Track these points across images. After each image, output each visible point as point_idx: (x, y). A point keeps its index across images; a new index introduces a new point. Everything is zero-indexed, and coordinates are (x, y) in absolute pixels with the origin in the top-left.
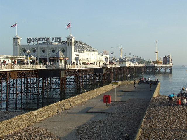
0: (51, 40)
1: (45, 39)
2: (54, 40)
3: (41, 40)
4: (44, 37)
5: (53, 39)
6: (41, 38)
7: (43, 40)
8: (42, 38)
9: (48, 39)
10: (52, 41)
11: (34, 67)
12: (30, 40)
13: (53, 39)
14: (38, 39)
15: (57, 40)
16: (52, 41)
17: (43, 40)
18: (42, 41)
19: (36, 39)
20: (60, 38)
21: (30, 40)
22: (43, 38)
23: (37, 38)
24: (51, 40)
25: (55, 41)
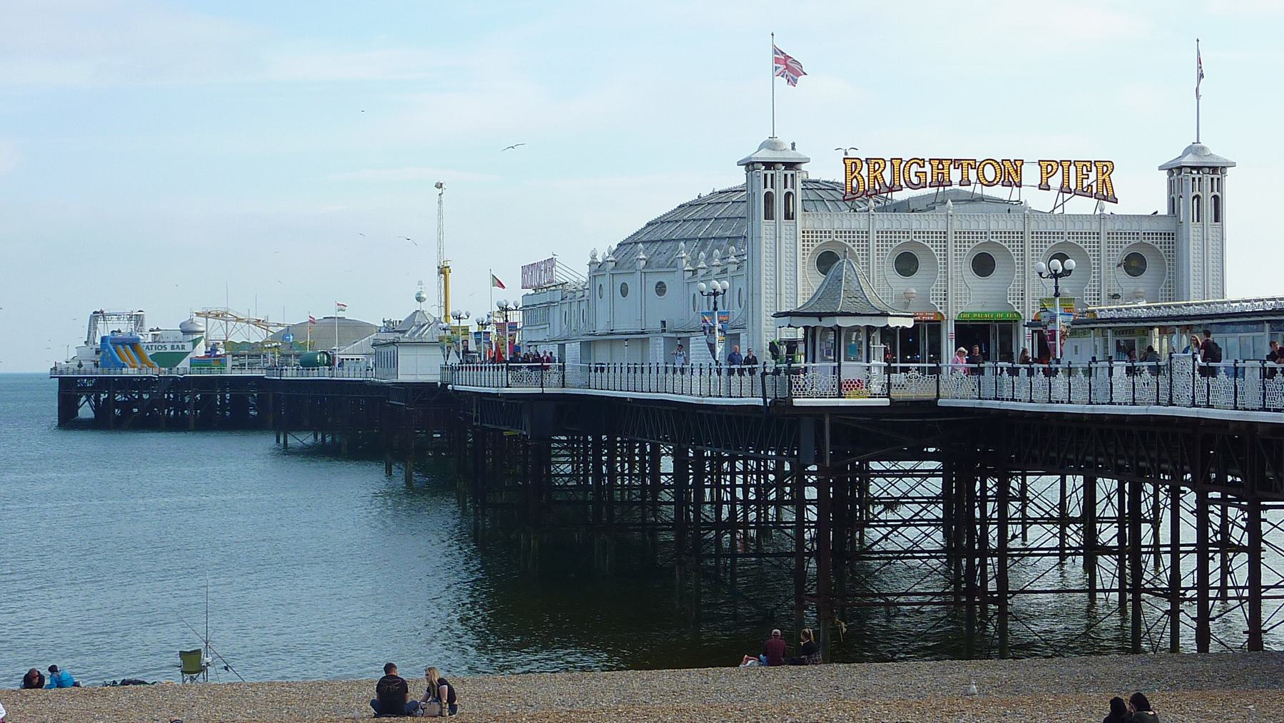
1: (990, 173)
3: (956, 175)
4: (979, 159)
5: (1048, 167)
6: (957, 163)
7: (973, 175)
9: (1010, 173)
11: (1100, 398)
12: (864, 172)
14: (928, 168)
18: (965, 182)
19: (915, 168)
20: (1106, 168)
21: (864, 172)
22: (973, 164)
23: (920, 162)
24: (1031, 175)
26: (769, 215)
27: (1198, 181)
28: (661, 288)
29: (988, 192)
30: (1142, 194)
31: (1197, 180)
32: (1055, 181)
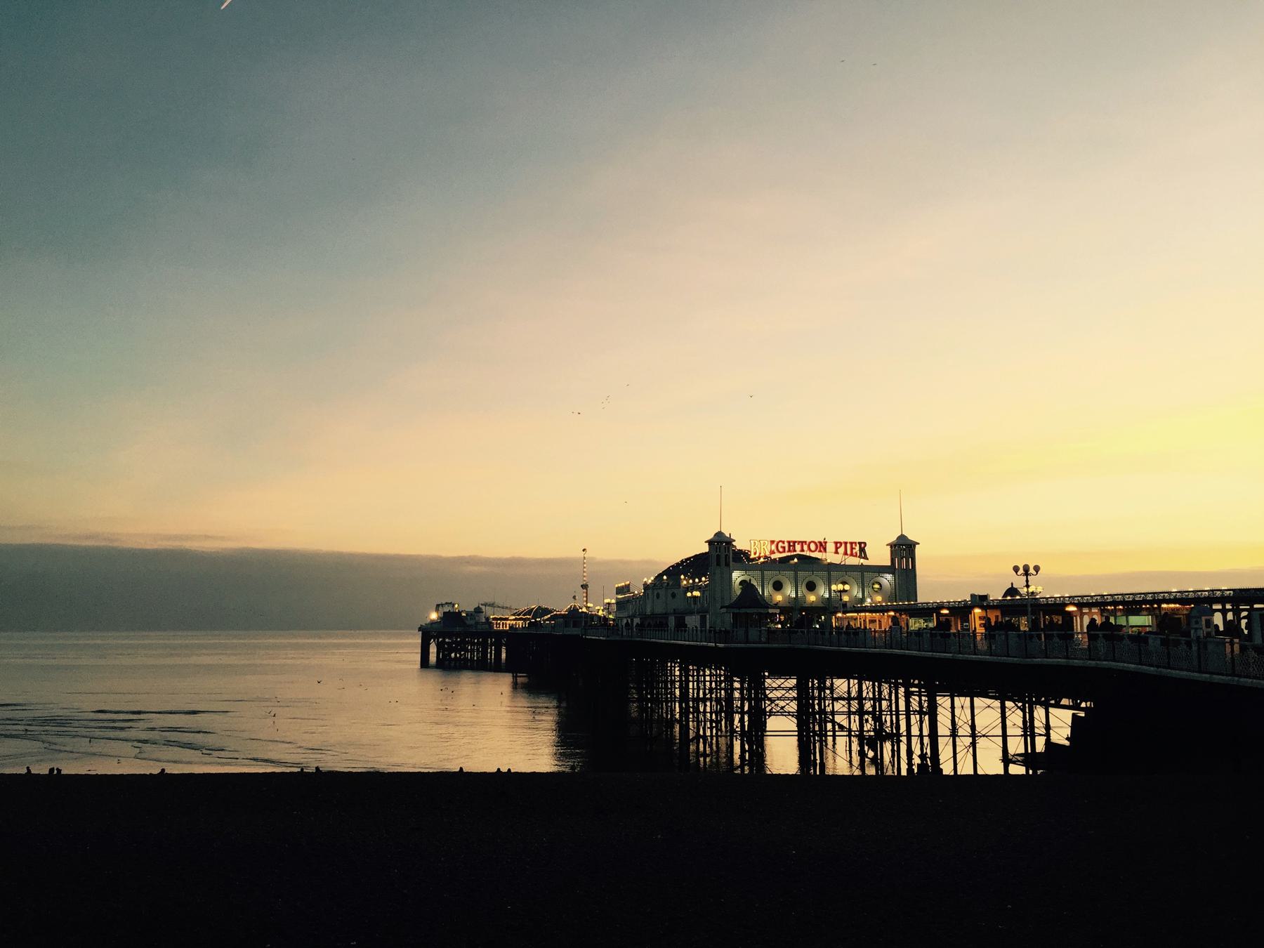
0: (831, 547)
1: (813, 547)
2: (841, 550)
3: (798, 547)
5: (837, 545)
7: (805, 547)
8: (802, 543)
9: (822, 546)
10: (836, 552)
13: (837, 548)
15: (852, 549)
16: (836, 552)
17: (805, 547)
18: (802, 550)
20: (862, 546)
24: (831, 547)
25: (846, 553)
26: (718, 564)
27: (904, 548)
28: (674, 596)
29: (813, 555)
30: (879, 555)
31: (904, 548)
32: (841, 550)
